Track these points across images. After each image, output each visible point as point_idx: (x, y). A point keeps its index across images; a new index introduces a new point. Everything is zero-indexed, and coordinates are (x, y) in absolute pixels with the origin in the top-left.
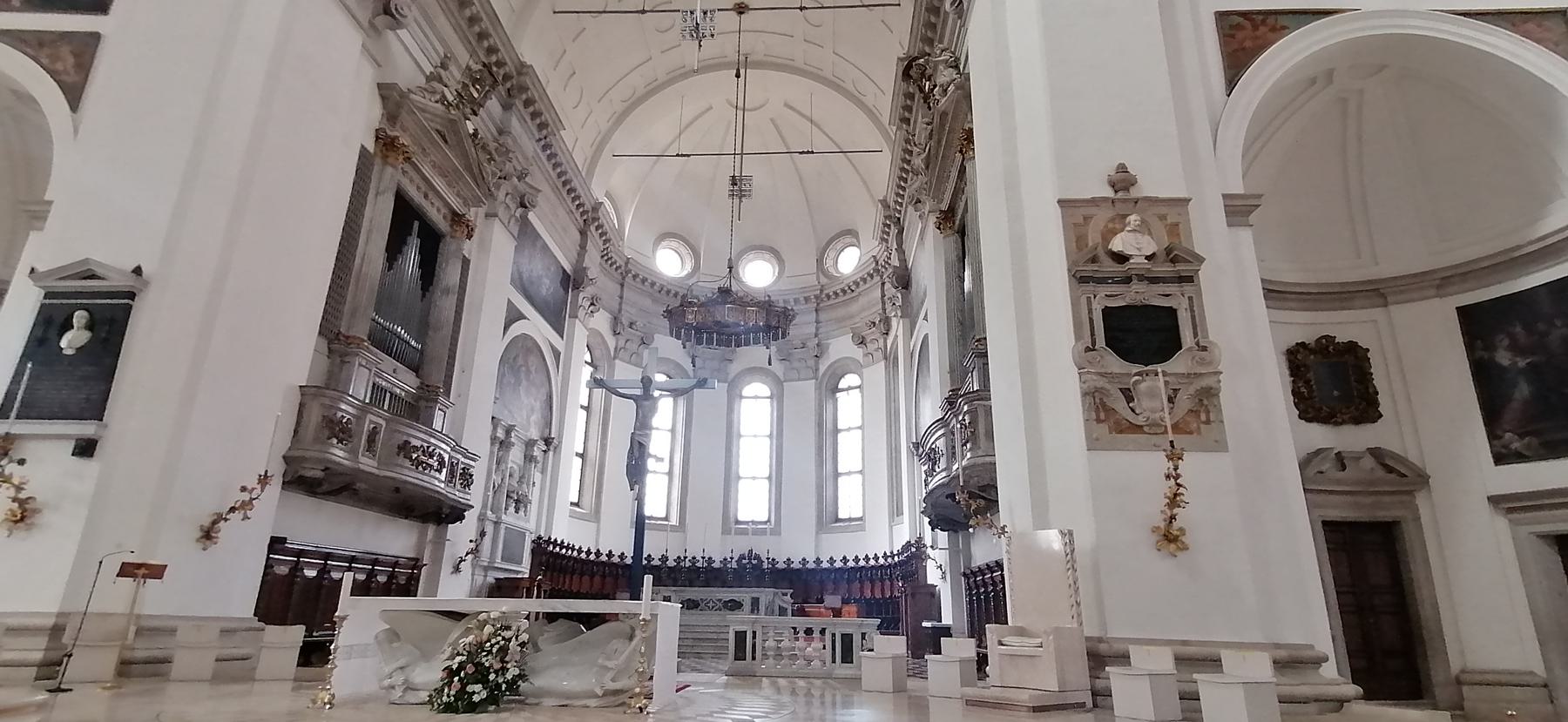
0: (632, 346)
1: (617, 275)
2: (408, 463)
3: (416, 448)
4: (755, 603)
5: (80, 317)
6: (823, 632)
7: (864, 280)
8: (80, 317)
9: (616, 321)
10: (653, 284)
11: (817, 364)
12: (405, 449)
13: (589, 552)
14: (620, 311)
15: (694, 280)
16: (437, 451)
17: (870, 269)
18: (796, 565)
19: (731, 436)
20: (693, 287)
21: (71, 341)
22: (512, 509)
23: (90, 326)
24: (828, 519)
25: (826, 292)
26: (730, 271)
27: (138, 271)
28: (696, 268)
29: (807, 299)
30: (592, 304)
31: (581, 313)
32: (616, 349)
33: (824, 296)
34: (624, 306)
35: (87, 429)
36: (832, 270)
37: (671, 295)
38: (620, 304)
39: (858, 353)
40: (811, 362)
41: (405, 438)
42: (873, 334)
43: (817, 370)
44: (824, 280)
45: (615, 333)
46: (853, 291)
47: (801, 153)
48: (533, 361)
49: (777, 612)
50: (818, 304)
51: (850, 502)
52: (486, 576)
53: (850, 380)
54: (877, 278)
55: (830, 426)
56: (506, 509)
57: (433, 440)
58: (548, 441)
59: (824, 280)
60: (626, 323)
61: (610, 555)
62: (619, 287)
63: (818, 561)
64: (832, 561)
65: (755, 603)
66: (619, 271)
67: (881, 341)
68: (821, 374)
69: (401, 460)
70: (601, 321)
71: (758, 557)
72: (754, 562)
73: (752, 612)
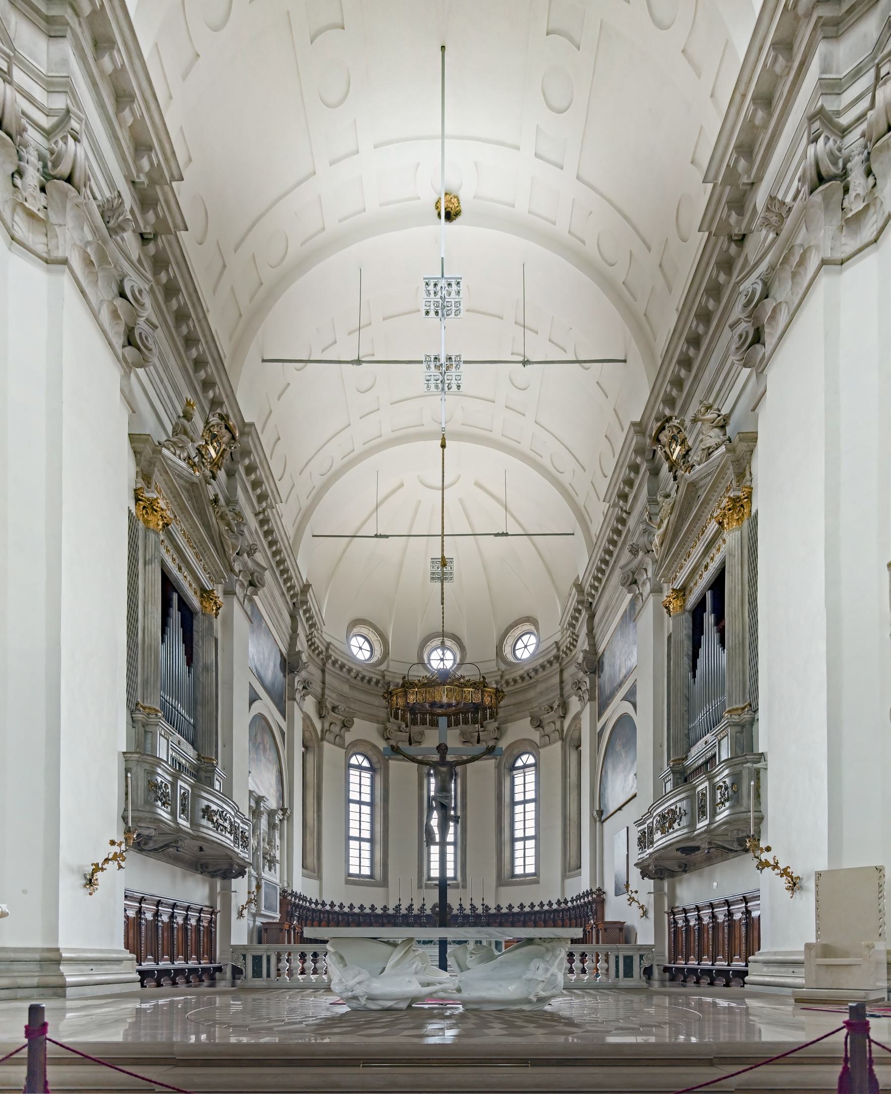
1: (318, 661)
2: (211, 826)
3: (216, 813)
9: (320, 704)
10: (350, 670)
12: (207, 811)
14: (323, 695)
16: (228, 815)
17: (550, 656)
20: (386, 673)
22: (267, 868)
25: (507, 677)
28: (386, 655)
30: (304, 688)
31: (298, 696)
33: (503, 682)
34: (327, 692)
36: (510, 658)
37: (365, 681)
38: (323, 689)
41: (206, 803)
44: (503, 667)
48: (268, 739)
52: (254, 921)
54: (556, 666)
55: (507, 799)
56: (264, 868)
57: (225, 806)
58: (284, 810)
59: (503, 667)
62: (319, 673)
66: (321, 656)
69: (204, 822)
70: (309, 704)
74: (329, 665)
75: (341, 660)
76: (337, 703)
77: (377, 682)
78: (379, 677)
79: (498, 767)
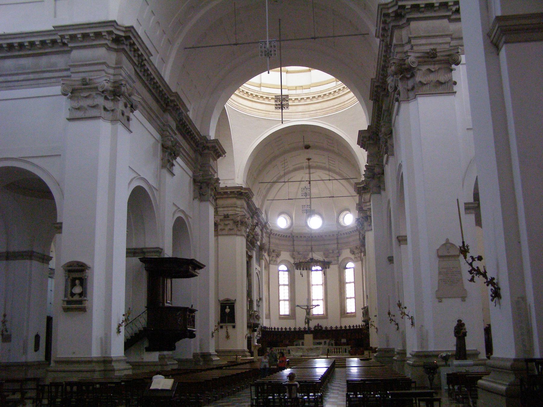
0: (274, 259)
4: (325, 342)
5: (228, 307)
6: (341, 348)
7: (354, 232)
8: (228, 307)
11: (338, 258)
13: (269, 328)
15: (291, 229)
18: (334, 329)
21: (228, 310)
23: (229, 308)
24: (343, 313)
26: (312, 249)
27: (235, 300)
29: (333, 235)
32: (269, 261)
34: (271, 245)
35: (233, 324)
38: (269, 244)
39: (352, 257)
40: (336, 258)
42: (356, 251)
43: (338, 261)
45: (269, 255)
46: (349, 234)
47: (330, 197)
49: (331, 344)
50: (337, 236)
51: (351, 307)
60: (272, 251)
61: (275, 328)
62: (268, 239)
63: (341, 327)
64: (345, 327)
65: (325, 342)
67: (360, 254)
68: (340, 262)
71: (321, 326)
72: (320, 328)
73: (325, 344)
74: (272, 236)
75: (275, 233)
76: (274, 248)
77: (289, 236)
78: (289, 235)
79: (339, 268)
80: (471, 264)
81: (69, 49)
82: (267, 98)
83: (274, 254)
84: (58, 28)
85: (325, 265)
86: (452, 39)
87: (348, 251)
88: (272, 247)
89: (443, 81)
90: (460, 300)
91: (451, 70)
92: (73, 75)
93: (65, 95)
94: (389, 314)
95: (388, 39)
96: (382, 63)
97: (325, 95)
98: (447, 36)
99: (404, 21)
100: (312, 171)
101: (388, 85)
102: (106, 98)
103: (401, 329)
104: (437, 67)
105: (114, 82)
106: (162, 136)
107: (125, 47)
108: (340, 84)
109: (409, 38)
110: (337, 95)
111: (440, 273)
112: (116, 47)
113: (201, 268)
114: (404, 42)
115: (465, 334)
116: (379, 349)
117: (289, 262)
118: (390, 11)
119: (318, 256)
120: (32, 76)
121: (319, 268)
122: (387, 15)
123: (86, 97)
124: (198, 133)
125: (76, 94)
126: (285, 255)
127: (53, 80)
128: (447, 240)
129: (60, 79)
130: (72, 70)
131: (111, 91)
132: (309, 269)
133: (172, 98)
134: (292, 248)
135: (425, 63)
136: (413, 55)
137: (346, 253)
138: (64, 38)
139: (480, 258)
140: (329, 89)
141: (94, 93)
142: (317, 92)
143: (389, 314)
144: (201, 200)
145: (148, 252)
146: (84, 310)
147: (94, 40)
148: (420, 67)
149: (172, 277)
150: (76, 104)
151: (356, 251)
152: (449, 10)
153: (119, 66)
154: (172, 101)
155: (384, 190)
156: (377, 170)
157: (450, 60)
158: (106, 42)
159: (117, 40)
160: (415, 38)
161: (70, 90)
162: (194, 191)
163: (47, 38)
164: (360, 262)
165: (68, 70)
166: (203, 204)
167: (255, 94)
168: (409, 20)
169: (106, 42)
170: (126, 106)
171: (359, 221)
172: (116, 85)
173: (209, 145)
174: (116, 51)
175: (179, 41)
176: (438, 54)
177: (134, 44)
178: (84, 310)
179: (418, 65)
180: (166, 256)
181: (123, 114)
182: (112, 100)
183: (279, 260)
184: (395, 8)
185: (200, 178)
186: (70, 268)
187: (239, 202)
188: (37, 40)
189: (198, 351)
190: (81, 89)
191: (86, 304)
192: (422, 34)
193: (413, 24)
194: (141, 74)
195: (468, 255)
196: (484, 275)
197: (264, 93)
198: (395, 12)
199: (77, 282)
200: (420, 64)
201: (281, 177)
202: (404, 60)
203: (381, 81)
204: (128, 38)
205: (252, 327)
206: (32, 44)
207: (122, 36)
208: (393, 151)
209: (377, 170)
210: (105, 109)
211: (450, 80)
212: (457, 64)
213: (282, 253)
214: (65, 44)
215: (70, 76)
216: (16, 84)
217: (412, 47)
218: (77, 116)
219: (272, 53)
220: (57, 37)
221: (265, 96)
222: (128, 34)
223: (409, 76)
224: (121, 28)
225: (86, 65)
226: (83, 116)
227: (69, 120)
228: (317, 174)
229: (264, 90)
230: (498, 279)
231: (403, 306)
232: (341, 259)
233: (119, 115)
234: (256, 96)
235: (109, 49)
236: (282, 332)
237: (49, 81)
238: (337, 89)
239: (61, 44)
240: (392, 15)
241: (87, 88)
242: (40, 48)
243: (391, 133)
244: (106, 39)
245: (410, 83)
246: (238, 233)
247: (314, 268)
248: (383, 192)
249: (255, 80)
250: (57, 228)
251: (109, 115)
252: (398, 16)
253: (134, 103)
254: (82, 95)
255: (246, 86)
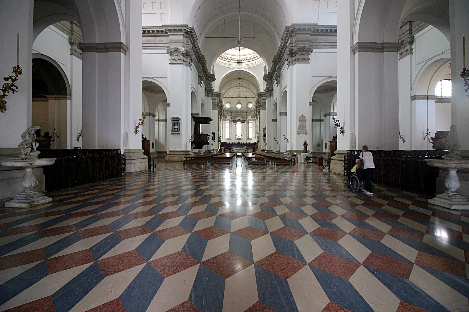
19: (236, 128)
24: (248, 138)
39: (252, 119)
42: (253, 117)
51: (250, 137)
53: (250, 122)
65: (243, 148)
80: (336, 123)
81: (168, 35)
82: (228, 59)
83: (225, 117)
84: (164, 26)
85: (243, 121)
86: (311, 42)
87: (250, 117)
88: (224, 114)
89: (306, 58)
90: (305, 134)
91: (309, 54)
92: (170, 46)
93: (168, 54)
94: (275, 138)
95: (286, 41)
96: (281, 49)
97: (249, 59)
98: (309, 41)
99: (294, 34)
100: (240, 87)
101: (284, 58)
102: (184, 56)
103: (279, 143)
104: (304, 53)
105: (186, 50)
106: (198, 72)
107: (190, 36)
108: (256, 54)
109: (296, 41)
110: (253, 59)
111: (299, 125)
112: (186, 36)
113: (211, 121)
114: (293, 42)
115: (307, 145)
116: (267, 150)
117: (229, 120)
118: (290, 30)
119: (241, 119)
120: (153, 45)
121: (240, 122)
122: (288, 31)
123: (176, 55)
124: (208, 72)
125: (172, 54)
126: (228, 117)
127: (162, 47)
128: (302, 114)
129: (166, 47)
130: (170, 44)
131: (185, 54)
132: (237, 122)
133: (202, 58)
134: (231, 115)
135: (300, 51)
136: (297, 48)
137: (249, 118)
138: (167, 30)
139: (338, 121)
140: (251, 57)
141: (179, 54)
142: (246, 58)
143: (275, 138)
144: (208, 97)
145: (194, 115)
146: (179, 134)
147: (178, 32)
148: (298, 53)
149: (201, 124)
150: (172, 58)
151: (253, 117)
152: (311, 31)
153: (188, 44)
154: (202, 59)
155: (272, 96)
156: (270, 89)
157: (309, 50)
158: (183, 33)
159: (187, 33)
160: (298, 41)
161: (170, 52)
162: (206, 93)
163: (160, 30)
164: (254, 121)
165: (169, 43)
166: (209, 98)
167: (223, 57)
168: (296, 34)
169: (183, 33)
170: (190, 60)
171: (256, 107)
172: (187, 51)
173: (211, 76)
174: (186, 37)
175: (204, 34)
176: (306, 48)
177: (193, 35)
178: (179, 134)
179: (298, 52)
180: (200, 116)
181: (190, 63)
182: (186, 57)
183: (226, 119)
184: (292, 29)
185: (208, 89)
186: (174, 119)
187: (216, 98)
188: (155, 30)
189: (207, 149)
190: (174, 52)
191: (180, 132)
192: (300, 40)
193: (297, 36)
194: (193, 47)
195: (335, 120)
196: (339, 126)
197: (226, 57)
198: (292, 30)
199: (176, 124)
200: (299, 51)
201: (229, 89)
202: (293, 49)
203: (278, 56)
204: (191, 32)
205: (220, 141)
206: (153, 31)
207: (189, 31)
208: (280, 83)
209: (270, 89)
210: (183, 60)
211: (309, 58)
212: (311, 52)
213: (228, 117)
214: (166, 33)
215: (169, 46)
216: (147, 47)
217: (296, 44)
218: (173, 63)
219: (241, 42)
220: (163, 29)
221: (227, 58)
222: (192, 31)
223: (294, 56)
224: (189, 28)
225: (175, 42)
226: (175, 63)
227: (170, 64)
228: (242, 89)
229: (226, 55)
230: (344, 127)
231: (285, 136)
232: (247, 119)
233: (188, 63)
234: (224, 58)
235: (184, 36)
236: (227, 144)
237: (160, 47)
238: (253, 57)
239: (165, 32)
240: (290, 31)
241: (176, 52)
242: (156, 34)
243: (280, 76)
244: (183, 32)
245: (294, 58)
246: (216, 109)
247: (238, 122)
248: (271, 97)
249: (228, 52)
250: (167, 105)
251: (185, 63)
252: (292, 32)
253: (193, 59)
254: (175, 54)
255: (223, 55)
